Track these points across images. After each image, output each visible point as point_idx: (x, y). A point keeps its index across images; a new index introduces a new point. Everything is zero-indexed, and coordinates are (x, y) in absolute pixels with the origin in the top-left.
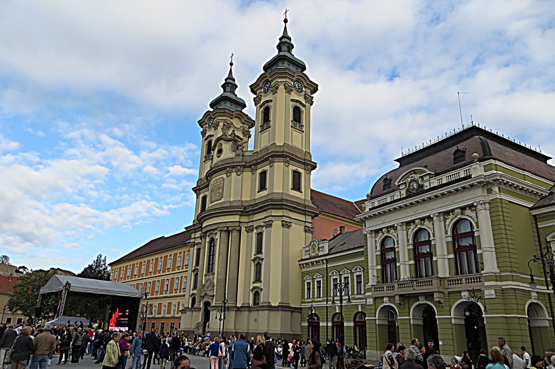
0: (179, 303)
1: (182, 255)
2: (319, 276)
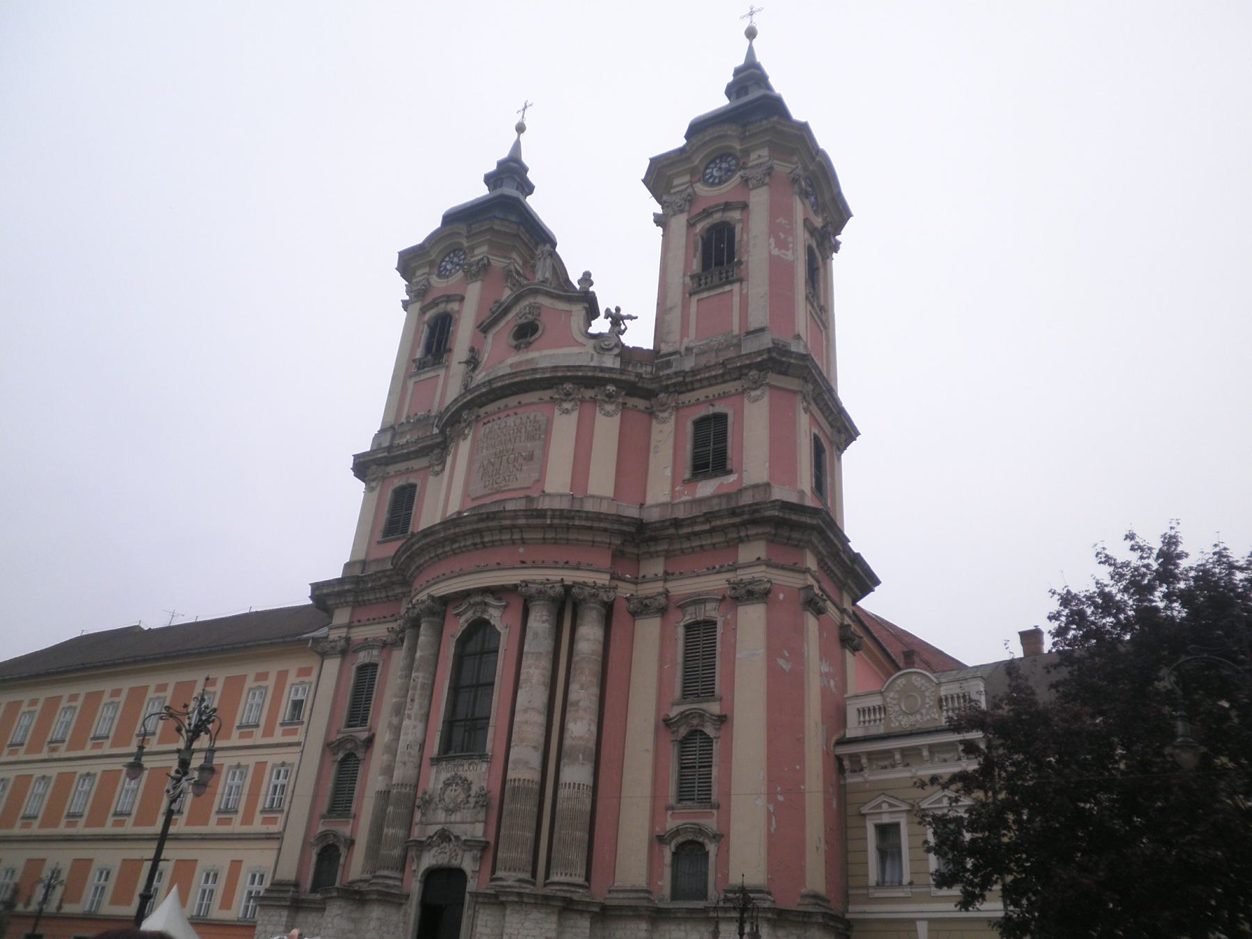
0: (236, 865)
1: (271, 682)
2: (891, 805)
